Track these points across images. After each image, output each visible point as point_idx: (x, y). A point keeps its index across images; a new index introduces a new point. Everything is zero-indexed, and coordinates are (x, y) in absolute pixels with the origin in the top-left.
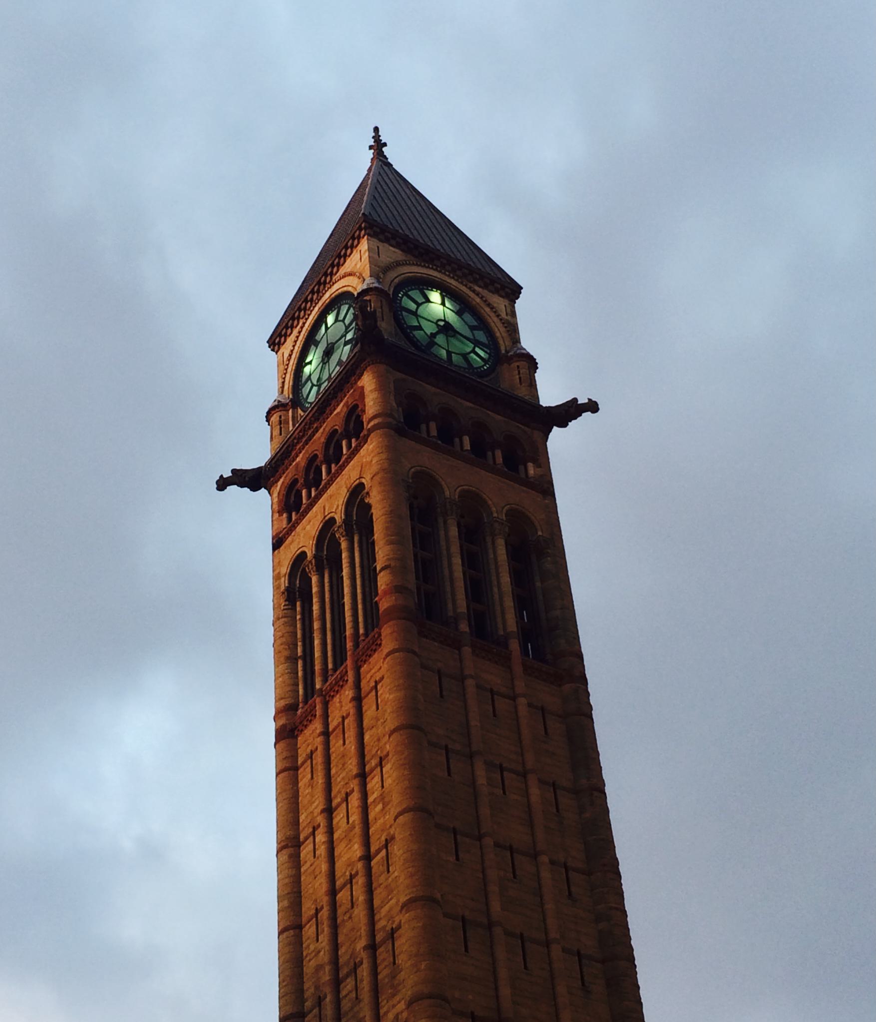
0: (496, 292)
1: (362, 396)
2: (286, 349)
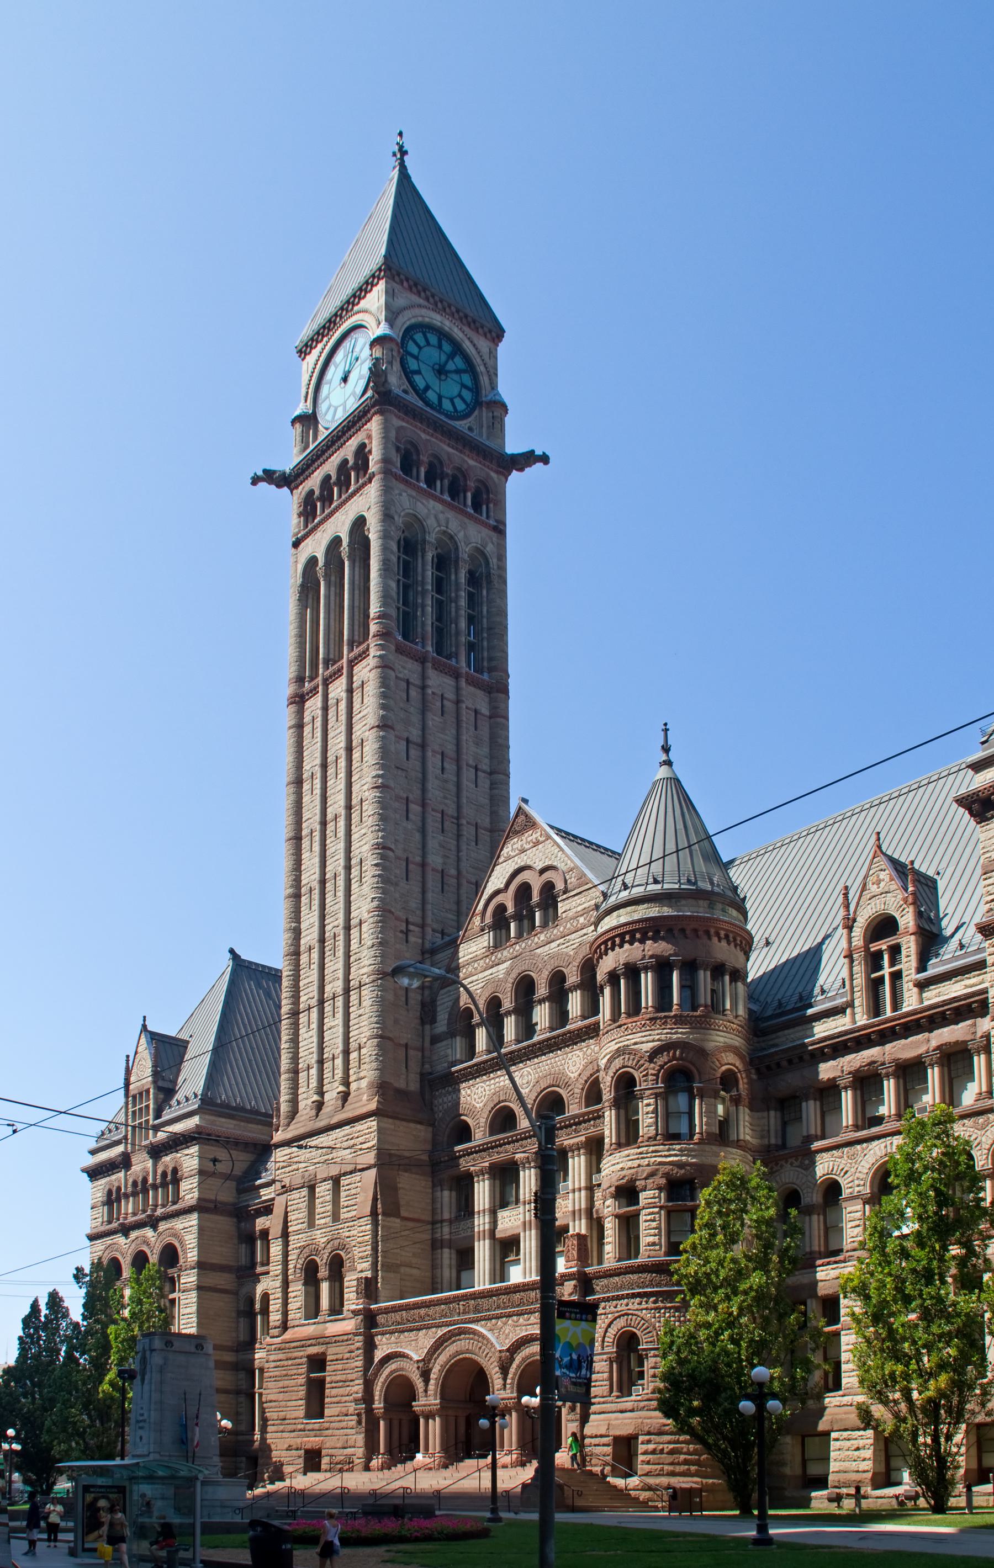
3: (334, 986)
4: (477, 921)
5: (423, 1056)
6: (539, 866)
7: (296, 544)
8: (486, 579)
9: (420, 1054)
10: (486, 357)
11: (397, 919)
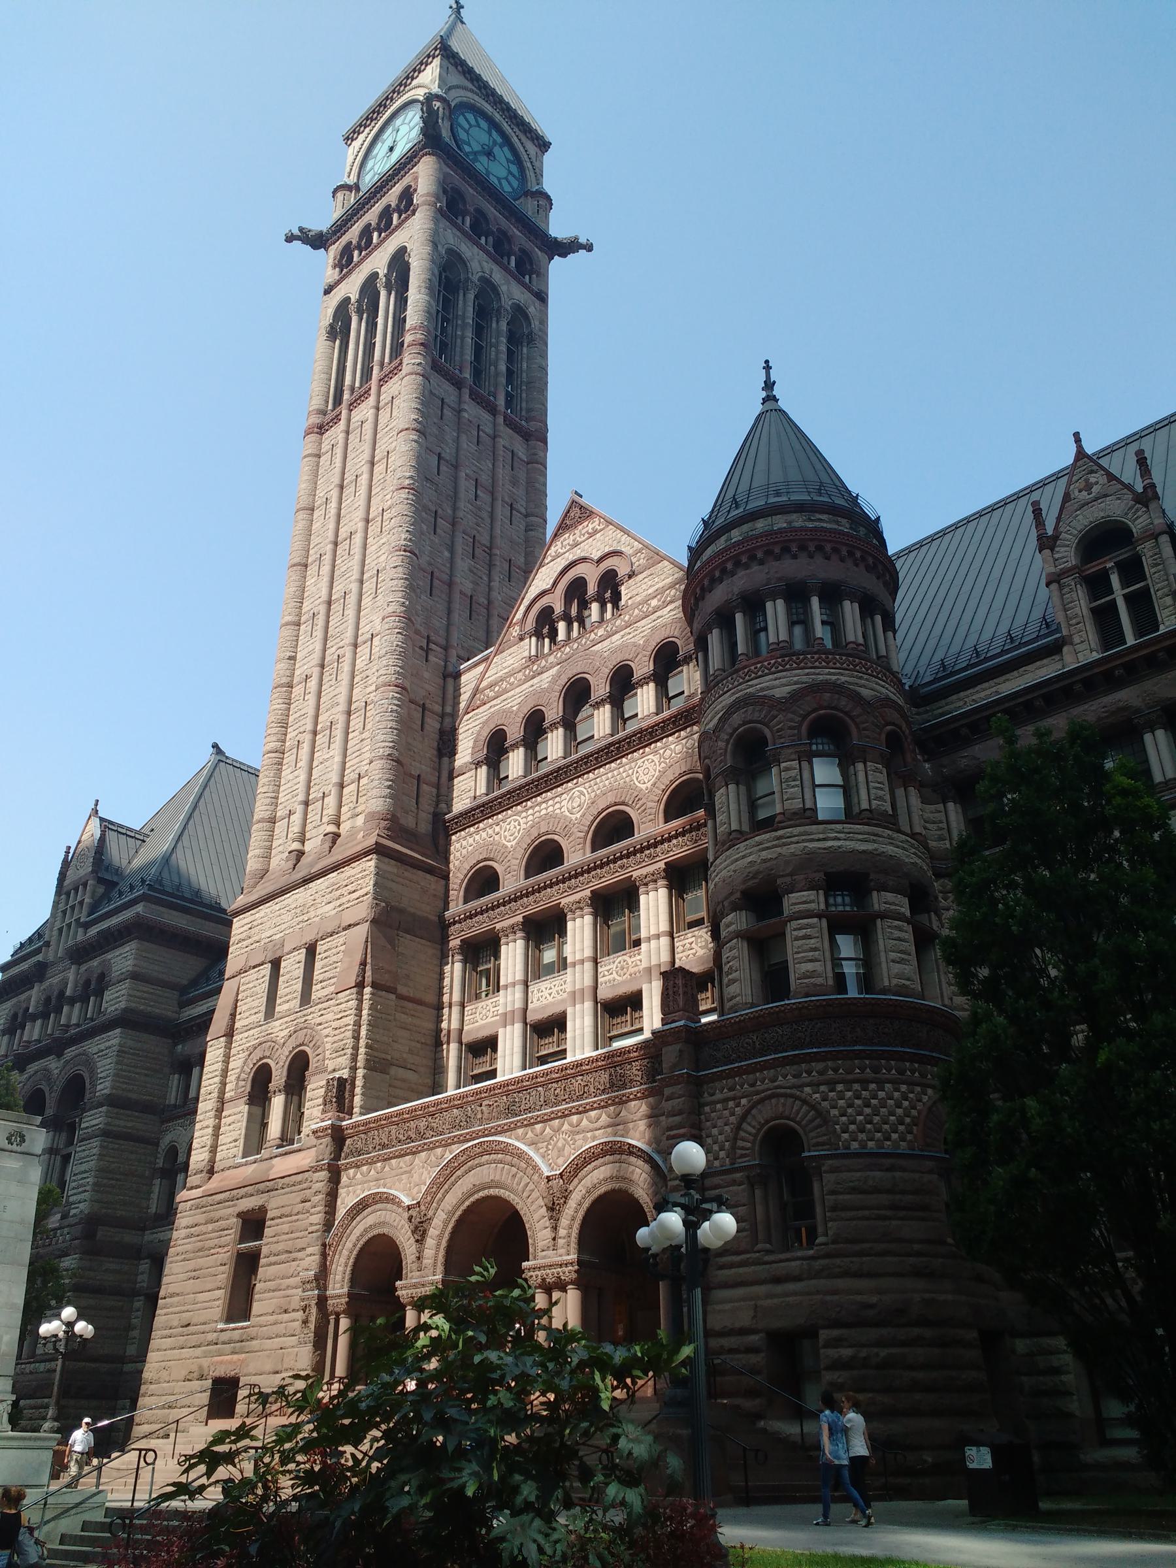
0: (532, 140)
1: (416, 179)
2: (356, 144)
3: (333, 713)
4: (515, 631)
5: (438, 796)
6: (596, 555)
7: (327, 292)
8: (527, 335)
9: (434, 791)
10: (534, 159)
11: (417, 632)
